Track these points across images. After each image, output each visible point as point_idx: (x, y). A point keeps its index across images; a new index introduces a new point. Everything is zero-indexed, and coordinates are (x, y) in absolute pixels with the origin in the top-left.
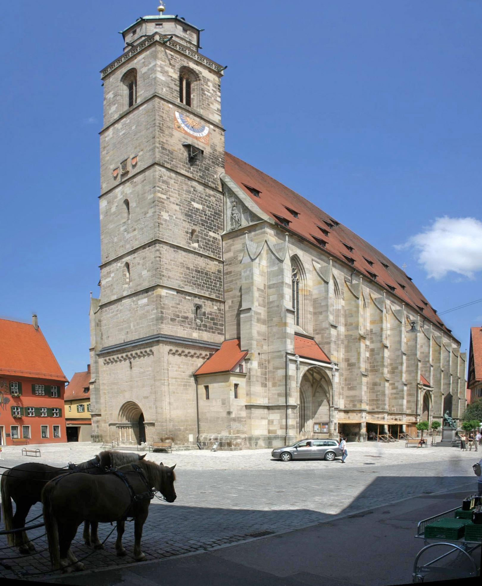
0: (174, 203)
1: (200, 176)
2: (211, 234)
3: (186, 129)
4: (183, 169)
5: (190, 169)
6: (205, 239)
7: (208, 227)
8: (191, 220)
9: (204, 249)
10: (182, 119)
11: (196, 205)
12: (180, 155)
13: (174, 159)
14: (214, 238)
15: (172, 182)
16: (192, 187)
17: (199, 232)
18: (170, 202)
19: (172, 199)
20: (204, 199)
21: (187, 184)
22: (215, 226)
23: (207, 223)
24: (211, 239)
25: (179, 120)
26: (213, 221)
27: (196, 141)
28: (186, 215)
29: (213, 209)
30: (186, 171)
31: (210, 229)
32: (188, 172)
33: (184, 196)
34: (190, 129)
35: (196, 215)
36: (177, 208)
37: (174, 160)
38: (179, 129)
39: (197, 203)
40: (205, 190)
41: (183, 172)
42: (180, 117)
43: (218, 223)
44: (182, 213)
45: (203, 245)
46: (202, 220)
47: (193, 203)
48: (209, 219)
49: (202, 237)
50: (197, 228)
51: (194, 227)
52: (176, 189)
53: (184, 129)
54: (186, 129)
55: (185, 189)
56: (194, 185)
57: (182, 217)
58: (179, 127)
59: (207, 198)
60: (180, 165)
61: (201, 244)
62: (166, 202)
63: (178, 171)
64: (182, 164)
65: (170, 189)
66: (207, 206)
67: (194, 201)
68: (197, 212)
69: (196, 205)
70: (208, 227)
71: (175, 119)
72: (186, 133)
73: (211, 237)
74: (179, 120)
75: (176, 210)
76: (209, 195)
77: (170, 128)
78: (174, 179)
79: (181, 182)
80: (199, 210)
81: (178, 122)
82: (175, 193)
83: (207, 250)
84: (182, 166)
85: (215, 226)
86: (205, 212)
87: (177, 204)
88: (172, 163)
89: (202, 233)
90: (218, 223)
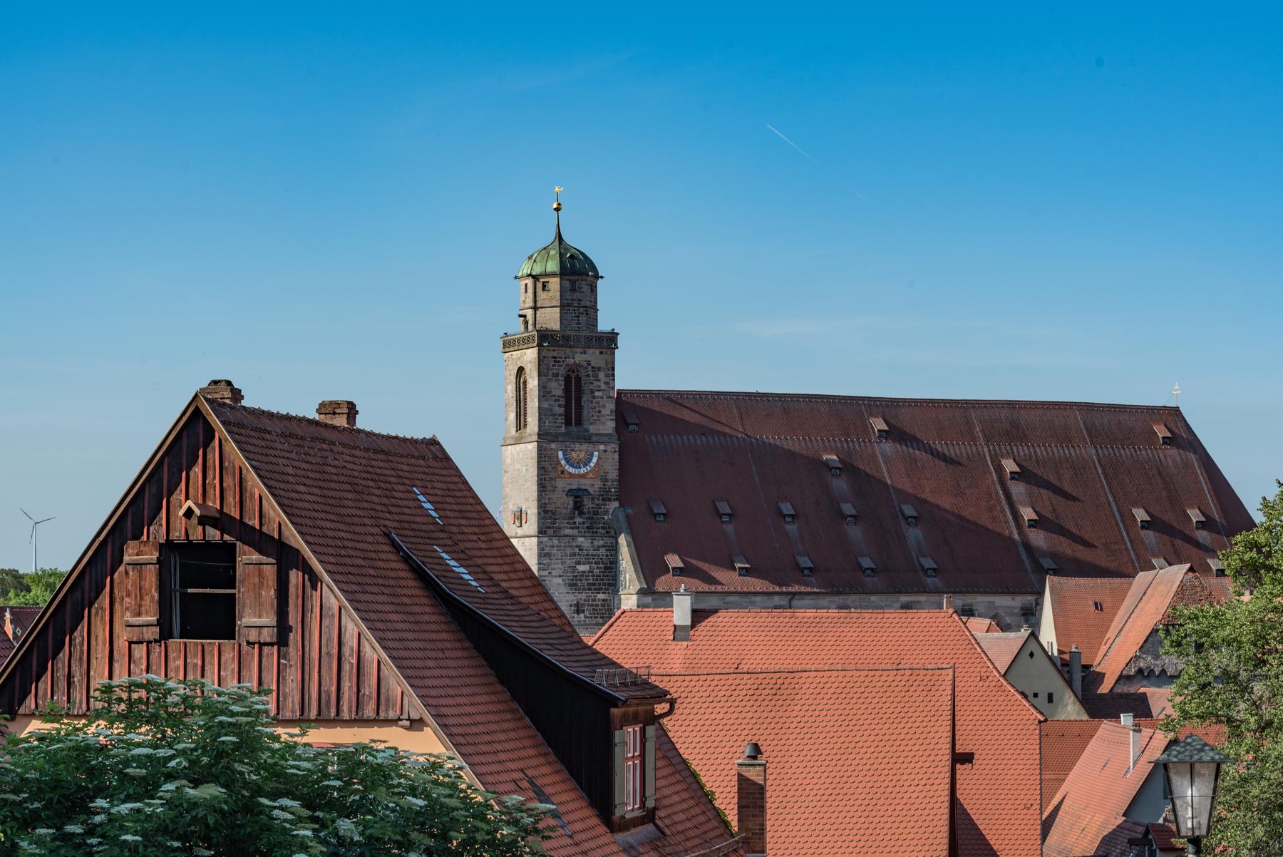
0: (556, 576)
1: (588, 527)
2: (601, 596)
3: (571, 470)
4: (567, 528)
5: (575, 523)
6: (592, 605)
7: (596, 589)
8: (576, 589)
9: (591, 617)
10: (565, 459)
11: (581, 568)
14: (603, 600)
15: (554, 551)
16: (577, 546)
17: (585, 600)
18: (552, 577)
19: (554, 573)
20: (592, 555)
22: (604, 585)
23: (594, 584)
24: (600, 603)
25: (563, 462)
26: (603, 580)
27: (583, 481)
28: (570, 585)
29: (603, 563)
30: (571, 528)
31: (598, 590)
32: (573, 528)
33: (568, 561)
34: (576, 468)
35: (581, 580)
36: (559, 580)
38: (562, 476)
39: (583, 564)
40: (592, 543)
41: (567, 531)
42: (564, 455)
43: (609, 580)
44: (566, 584)
45: (590, 614)
46: (589, 584)
47: (578, 567)
48: (597, 580)
49: (589, 605)
50: (583, 596)
51: (580, 596)
53: (569, 473)
54: (571, 470)
55: (568, 553)
57: (564, 589)
58: (563, 472)
59: (595, 552)
61: (587, 613)
62: (547, 578)
66: (596, 563)
67: (579, 563)
68: (583, 576)
69: (581, 568)
70: (596, 589)
71: (558, 462)
72: (572, 476)
73: (599, 600)
74: (563, 462)
75: (558, 584)
76: (598, 547)
77: (551, 479)
78: (557, 546)
80: (585, 572)
81: (561, 466)
83: (595, 617)
85: (604, 585)
86: (593, 572)
87: (560, 576)
89: (589, 601)
90: (609, 580)
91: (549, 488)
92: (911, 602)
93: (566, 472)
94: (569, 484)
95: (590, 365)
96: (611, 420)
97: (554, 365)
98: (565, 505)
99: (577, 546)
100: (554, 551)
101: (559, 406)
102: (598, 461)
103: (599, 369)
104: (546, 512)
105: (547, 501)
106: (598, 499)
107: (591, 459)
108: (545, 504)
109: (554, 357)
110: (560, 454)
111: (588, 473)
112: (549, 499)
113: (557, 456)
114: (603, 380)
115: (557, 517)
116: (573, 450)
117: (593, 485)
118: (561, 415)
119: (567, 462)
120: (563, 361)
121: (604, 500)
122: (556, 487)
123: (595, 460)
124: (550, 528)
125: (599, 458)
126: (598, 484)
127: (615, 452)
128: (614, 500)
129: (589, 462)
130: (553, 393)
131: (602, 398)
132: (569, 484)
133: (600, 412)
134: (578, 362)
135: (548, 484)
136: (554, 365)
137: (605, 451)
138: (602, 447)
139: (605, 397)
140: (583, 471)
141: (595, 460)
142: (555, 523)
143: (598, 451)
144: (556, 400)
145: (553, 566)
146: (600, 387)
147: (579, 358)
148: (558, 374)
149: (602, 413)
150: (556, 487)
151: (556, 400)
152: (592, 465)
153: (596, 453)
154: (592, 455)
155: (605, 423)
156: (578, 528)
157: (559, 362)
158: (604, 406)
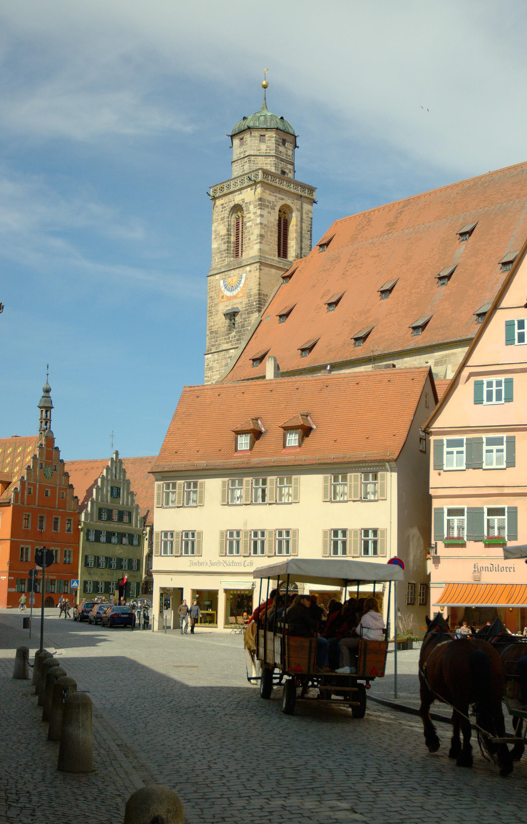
1: (238, 340)
3: (228, 294)
5: (229, 338)
12: (222, 329)
13: (218, 338)
15: (215, 365)
21: (226, 358)
27: (235, 301)
30: (227, 343)
37: (218, 339)
38: (222, 300)
41: (225, 346)
42: (224, 282)
52: (218, 369)
53: (226, 296)
54: (228, 294)
55: (224, 365)
56: (230, 355)
60: (221, 340)
63: (221, 350)
64: (224, 337)
65: (213, 373)
71: (220, 290)
79: (222, 359)
81: (222, 292)
82: (217, 374)
84: (224, 341)
88: (217, 343)
91: (214, 313)
92: (446, 356)
93: (224, 297)
94: (226, 306)
95: (243, 202)
96: (257, 243)
97: (222, 211)
98: (224, 325)
99: (229, 358)
100: (215, 365)
101: (224, 243)
102: (245, 281)
103: (250, 203)
104: (211, 333)
105: (212, 324)
106: (245, 313)
107: (240, 281)
108: (211, 326)
109: (222, 205)
110: (222, 282)
111: (238, 293)
112: (214, 322)
113: (220, 285)
114: (252, 212)
115: (218, 335)
116: (229, 277)
117: (241, 303)
118: (225, 250)
119: (226, 288)
120: (228, 206)
121: (248, 313)
122: (218, 311)
123: (243, 281)
124: (213, 346)
125: (246, 279)
126: (245, 300)
127: (257, 270)
128: (255, 312)
129: (239, 284)
130: (221, 234)
131: (251, 227)
132: (226, 306)
133: (249, 239)
134: (236, 203)
135: (213, 310)
136: (222, 211)
137: (250, 271)
138: (248, 268)
139: (253, 225)
140: (235, 293)
141: (243, 281)
142: (217, 341)
143: (246, 272)
144: (223, 239)
145: (214, 377)
146: (250, 218)
147: (237, 198)
148: (224, 218)
149: (251, 239)
150: (218, 311)
151: (223, 239)
152: (241, 285)
153: (244, 275)
154: (241, 278)
155: (253, 248)
156: (231, 342)
157: (225, 207)
158: (252, 234)
